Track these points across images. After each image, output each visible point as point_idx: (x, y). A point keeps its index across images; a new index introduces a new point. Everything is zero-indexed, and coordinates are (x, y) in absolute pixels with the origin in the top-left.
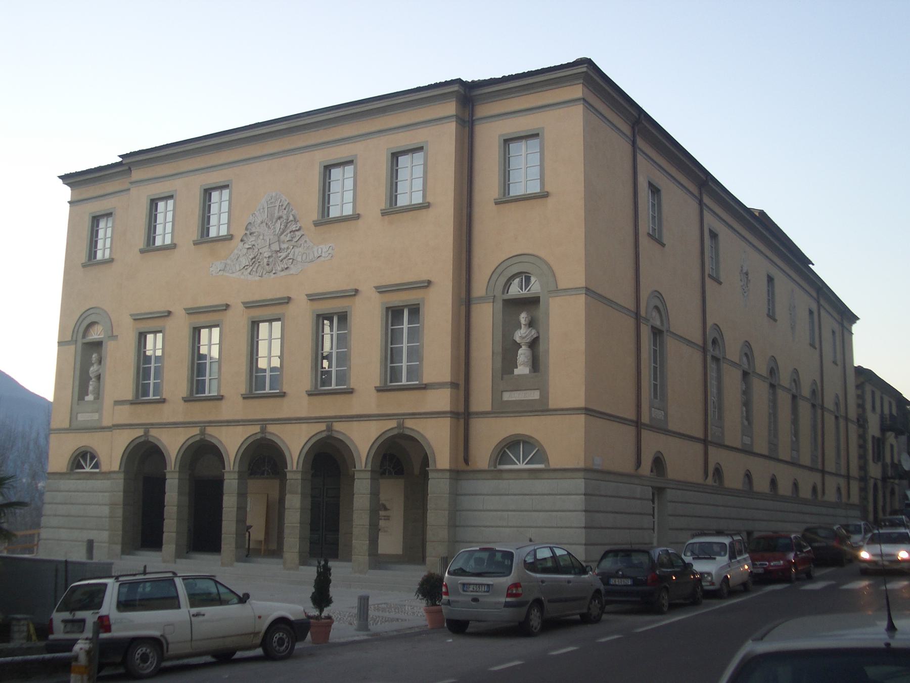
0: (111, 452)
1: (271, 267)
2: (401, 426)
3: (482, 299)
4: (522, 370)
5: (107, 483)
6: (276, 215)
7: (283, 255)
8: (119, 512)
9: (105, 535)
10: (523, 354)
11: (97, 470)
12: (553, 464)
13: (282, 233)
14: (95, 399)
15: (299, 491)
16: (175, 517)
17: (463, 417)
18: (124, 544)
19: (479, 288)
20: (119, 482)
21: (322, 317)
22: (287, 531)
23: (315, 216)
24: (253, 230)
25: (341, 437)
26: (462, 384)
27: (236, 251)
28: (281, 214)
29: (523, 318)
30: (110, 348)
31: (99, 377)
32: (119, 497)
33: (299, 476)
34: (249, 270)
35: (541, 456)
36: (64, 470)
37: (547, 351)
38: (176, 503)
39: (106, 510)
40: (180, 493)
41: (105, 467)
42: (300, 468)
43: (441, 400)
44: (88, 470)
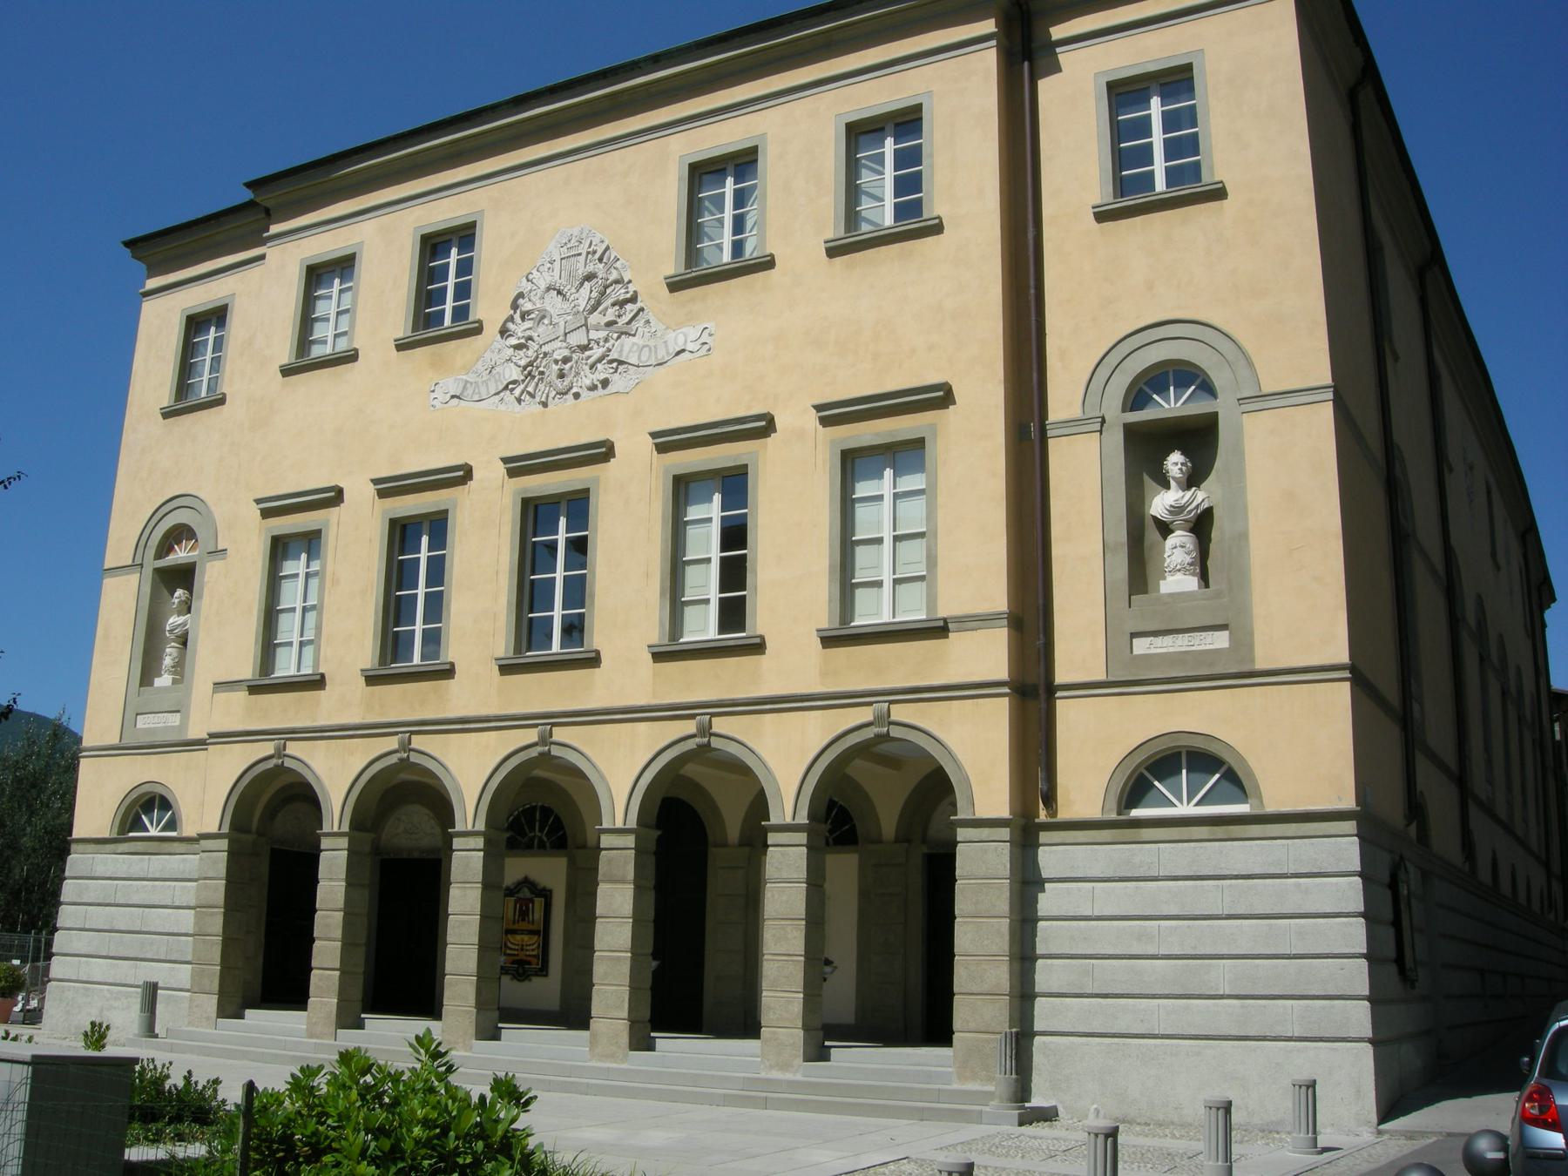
0: (204, 794)
1: (567, 381)
2: (884, 719)
3: (1073, 426)
4: (1176, 578)
5: (187, 863)
6: (581, 271)
7: (597, 352)
8: (216, 923)
10: (1177, 548)
11: (174, 834)
12: (1271, 807)
13: (594, 309)
14: (175, 682)
15: (631, 876)
16: (338, 933)
17: (1033, 693)
18: (222, 994)
19: (1064, 396)
20: (216, 861)
21: (684, 488)
22: (963, 903)
23: (672, 265)
24: (527, 306)
25: (733, 749)
26: (1031, 618)
27: (488, 355)
28: (590, 268)
29: (1175, 462)
30: (211, 577)
31: (184, 640)
32: (217, 891)
33: (630, 841)
34: (517, 392)
35: (1235, 782)
36: (106, 833)
37: (1243, 536)
38: (341, 904)
39: (187, 920)
40: (351, 882)
41: (188, 829)
42: (632, 822)
43: (987, 655)
44: (153, 832)
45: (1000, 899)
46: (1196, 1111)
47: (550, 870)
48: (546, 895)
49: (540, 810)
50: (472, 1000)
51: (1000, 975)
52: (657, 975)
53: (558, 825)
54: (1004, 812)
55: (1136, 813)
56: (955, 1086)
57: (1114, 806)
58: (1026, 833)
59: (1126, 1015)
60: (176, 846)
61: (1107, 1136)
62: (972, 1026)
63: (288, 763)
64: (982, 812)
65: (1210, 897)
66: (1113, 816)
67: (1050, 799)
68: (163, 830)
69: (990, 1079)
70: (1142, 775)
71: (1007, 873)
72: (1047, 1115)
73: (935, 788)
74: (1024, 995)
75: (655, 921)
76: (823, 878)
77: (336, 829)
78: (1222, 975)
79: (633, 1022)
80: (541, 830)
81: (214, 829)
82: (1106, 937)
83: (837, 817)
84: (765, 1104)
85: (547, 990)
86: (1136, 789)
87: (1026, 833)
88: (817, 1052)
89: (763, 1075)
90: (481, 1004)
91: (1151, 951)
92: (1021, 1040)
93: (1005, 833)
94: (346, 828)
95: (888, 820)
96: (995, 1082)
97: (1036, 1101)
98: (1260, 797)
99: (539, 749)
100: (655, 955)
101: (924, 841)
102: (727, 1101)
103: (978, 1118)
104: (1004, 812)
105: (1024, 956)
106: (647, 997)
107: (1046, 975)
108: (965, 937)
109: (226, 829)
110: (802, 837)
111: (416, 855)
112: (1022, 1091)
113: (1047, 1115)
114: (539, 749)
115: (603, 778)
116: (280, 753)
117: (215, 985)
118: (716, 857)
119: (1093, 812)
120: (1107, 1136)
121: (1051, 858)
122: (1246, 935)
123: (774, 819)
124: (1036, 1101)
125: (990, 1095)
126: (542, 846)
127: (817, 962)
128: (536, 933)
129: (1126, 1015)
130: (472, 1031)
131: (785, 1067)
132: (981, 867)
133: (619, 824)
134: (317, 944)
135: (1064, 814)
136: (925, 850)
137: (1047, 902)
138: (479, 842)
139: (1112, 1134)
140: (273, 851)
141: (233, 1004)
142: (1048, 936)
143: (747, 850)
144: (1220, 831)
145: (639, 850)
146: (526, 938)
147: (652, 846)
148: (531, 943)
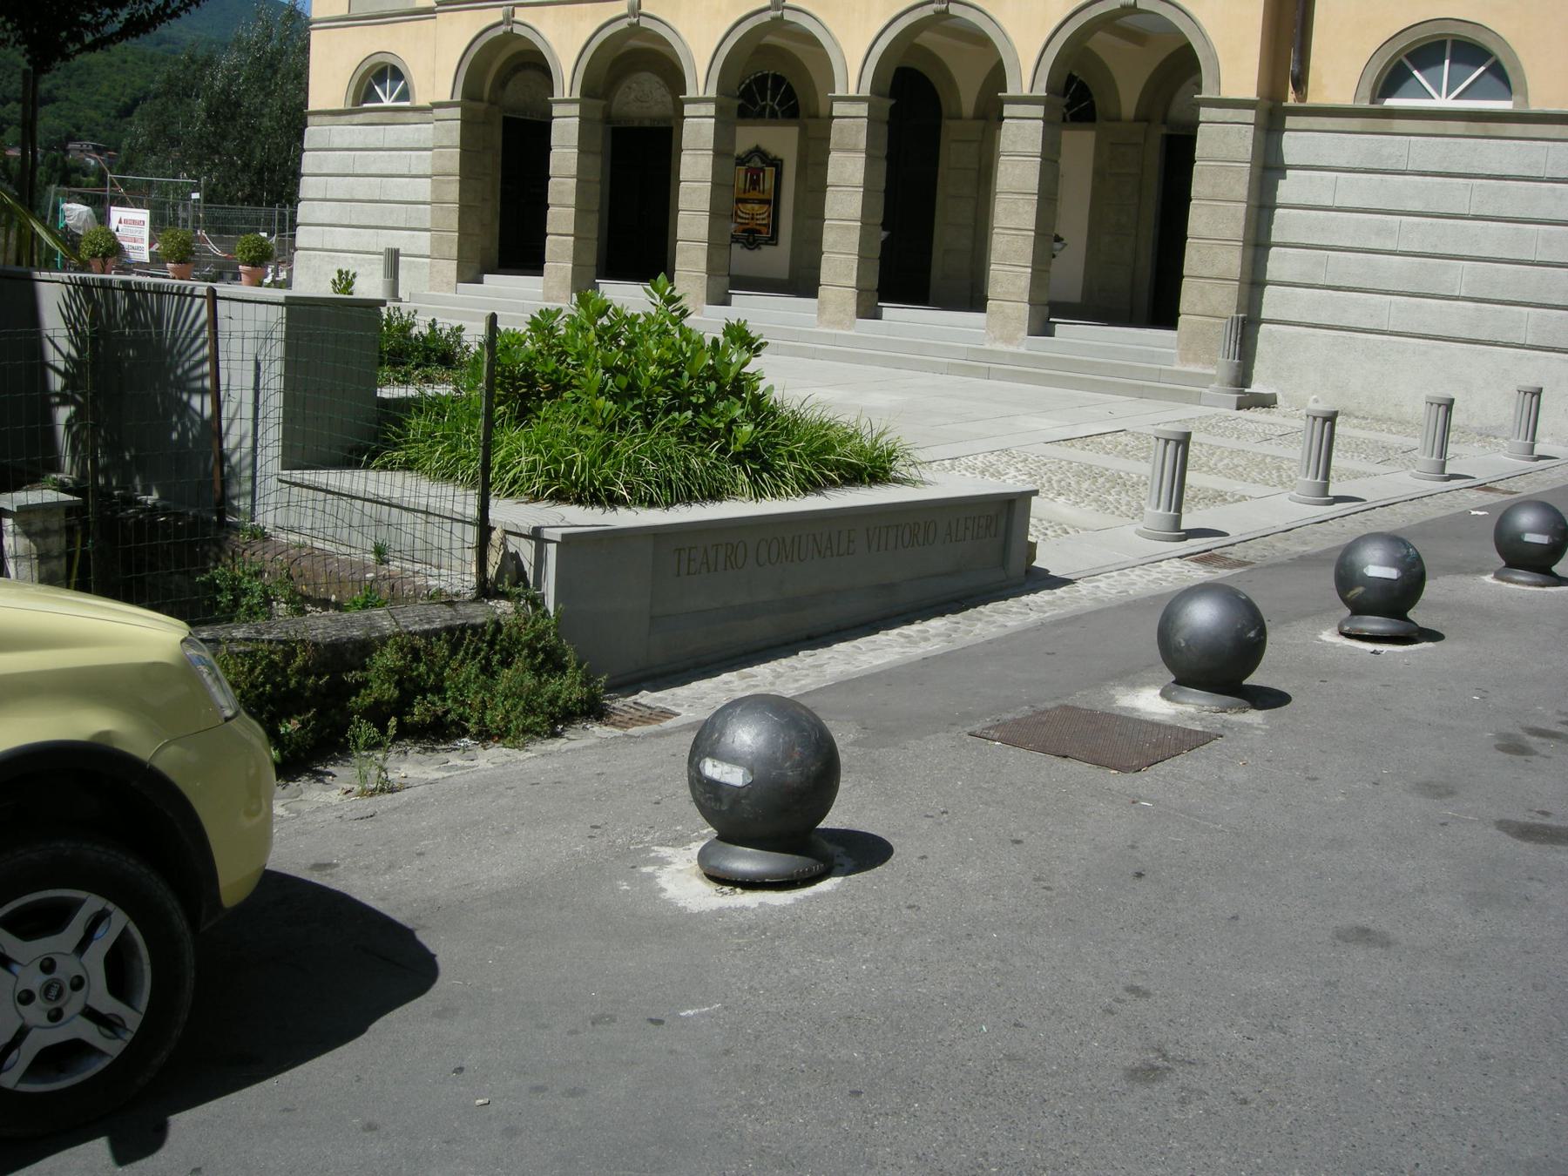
5: (421, 132)
8: (453, 190)
9: (423, 242)
11: (407, 104)
12: (1535, 106)
15: (863, 144)
16: (572, 200)
18: (462, 260)
20: (449, 129)
33: (862, 109)
35: (1500, 76)
36: (340, 105)
38: (574, 171)
41: (421, 98)
42: (866, 91)
45: (1238, 184)
46: (1417, 408)
47: (780, 140)
48: (777, 164)
49: (773, 78)
50: (703, 266)
51: (1232, 261)
52: (885, 245)
53: (790, 94)
54: (1251, 93)
55: (1390, 103)
56: (1177, 367)
57: (1368, 94)
58: (1271, 118)
59: (1356, 309)
60: (410, 116)
61: (1325, 420)
62: (1199, 309)
63: (517, 30)
64: (1227, 92)
65: (1458, 195)
66: (1366, 104)
67: (1300, 83)
68: (397, 100)
69: (1212, 363)
70: (1401, 62)
71: (1249, 157)
72: (1266, 402)
73: (1181, 65)
74: (1254, 282)
75: (887, 191)
76: (1059, 153)
77: (567, 96)
78: (1460, 277)
79: (861, 291)
80: (773, 99)
81: (446, 98)
82: (1346, 229)
83: (1075, 94)
84: (988, 374)
85: (776, 258)
86: (1393, 78)
87: (1271, 118)
88: (1042, 328)
89: (987, 346)
90: (712, 270)
91: (1390, 247)
92: (1247, 326)
93: (1250, 115)
94: (577, 95)
95: (1129, 99)
96: (1220, 366)
97: (1256, 387)
98: (1525, 95)
99: (772, 13)
100: (885, 226)
101: (1164, 122)
102: (951, 369)
103: (1197, 399)
104: (1251, 93)
105: (1258, 243)
106: (875, 266)
107: (1279, 264)
108: (1199, 219)
109: (458, 98)
110: (1039, 111)
111: (647, 124)
112: (1243, 377)
113: (1266, 402)
114: (772, 13)
115: (837, 44)
116: (509, 19)
117: (454, 252)
118: (949, 128)
119: (1345, 99)
120: (1325, 420)
121: (1295, 144)
122: (1492, 238)
123: (1011, 91)
124: (1256, 387)
125: (1212, 378)
126: (773, 115)
127: (1047, 238)
128: (767, 202)
129: (1356, 309)
130: (703, 295)
131: (1009, 340)
132: (1223, 149)
133: (852, 92)
134: (551, 211)
135: (1314, 98)
136: (1164, 130)
137: (1287, 189)
138: (711, 109)
139: (1331, 419)
140: (505, 118)
141: (471, 271)
142: (1284, 224)
143: (980, 123)
144: (1477, 127)
145: (872, 119)
146: (756, 207)
147: (885, 116)
148: (761, 213)
